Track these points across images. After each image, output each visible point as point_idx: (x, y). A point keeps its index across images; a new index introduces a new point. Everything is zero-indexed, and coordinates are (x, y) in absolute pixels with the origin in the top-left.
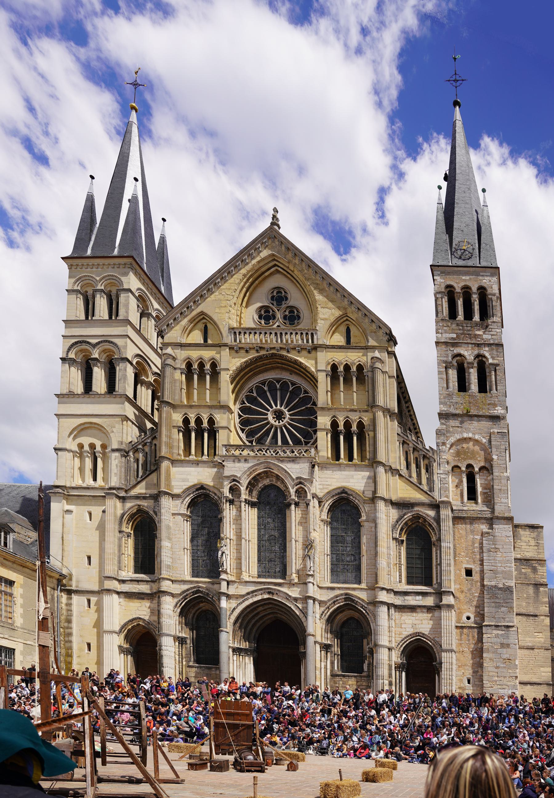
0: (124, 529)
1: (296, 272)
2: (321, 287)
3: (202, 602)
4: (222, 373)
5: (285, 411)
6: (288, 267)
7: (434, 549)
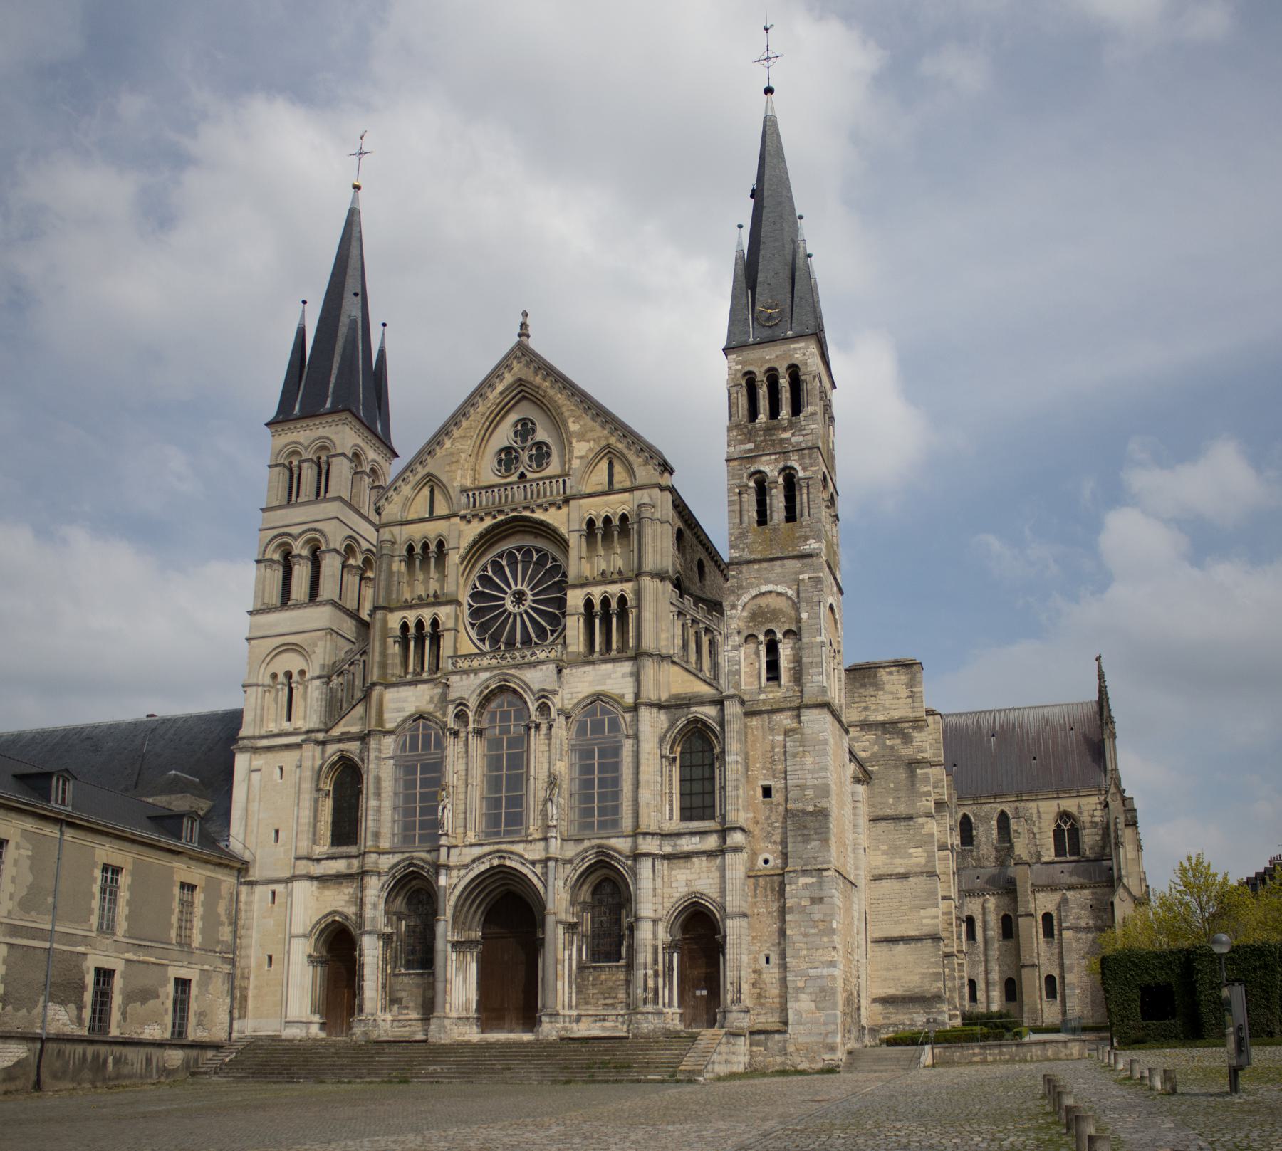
0: (321, 786)
3: (415, 878)
4: (451, 552)
5: (529, 593)
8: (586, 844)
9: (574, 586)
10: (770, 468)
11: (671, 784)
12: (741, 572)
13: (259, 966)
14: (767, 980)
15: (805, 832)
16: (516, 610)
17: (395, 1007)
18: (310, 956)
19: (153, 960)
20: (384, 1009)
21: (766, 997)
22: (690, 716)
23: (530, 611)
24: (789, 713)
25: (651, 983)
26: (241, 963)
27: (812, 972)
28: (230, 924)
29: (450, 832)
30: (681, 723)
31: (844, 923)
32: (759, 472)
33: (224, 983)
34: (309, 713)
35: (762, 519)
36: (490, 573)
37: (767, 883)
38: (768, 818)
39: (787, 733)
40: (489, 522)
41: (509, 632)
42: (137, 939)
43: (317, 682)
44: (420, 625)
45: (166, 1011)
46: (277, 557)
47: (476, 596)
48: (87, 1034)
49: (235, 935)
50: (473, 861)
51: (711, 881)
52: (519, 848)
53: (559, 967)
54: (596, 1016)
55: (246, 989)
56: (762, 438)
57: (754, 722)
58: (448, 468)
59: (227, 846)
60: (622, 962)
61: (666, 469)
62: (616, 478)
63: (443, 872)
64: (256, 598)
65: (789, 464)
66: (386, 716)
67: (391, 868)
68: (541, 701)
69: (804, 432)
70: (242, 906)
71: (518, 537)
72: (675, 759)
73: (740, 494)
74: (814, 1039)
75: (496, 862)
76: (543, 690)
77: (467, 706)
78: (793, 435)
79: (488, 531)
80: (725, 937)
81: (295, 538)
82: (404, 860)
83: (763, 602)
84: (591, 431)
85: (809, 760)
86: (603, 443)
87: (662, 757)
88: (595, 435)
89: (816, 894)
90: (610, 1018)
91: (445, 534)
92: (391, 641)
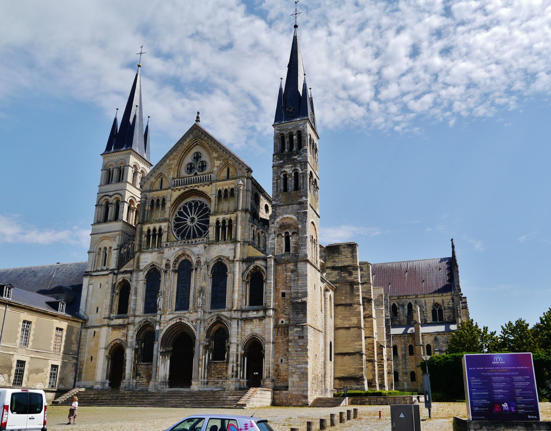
1: (205, 144)
2: (216, 150)
6: (202, 142)
7: (264, 284)
8: (213, 314)
9: (213, 215)
10: (288, 169)
11: (246, 291)
12: (276, 210)
13: (87, 360)
14: (281, 369)
15: (297, 311)
16: (191, 225)
17: (138, 377)
18: (107, 356)
19: (42, 357)
20: (133, 378)
21: (280, 376)
22: (254, 265)
23: (196, 225)
24: (293, 264)
25: (235, 369)
26: (81, 359)
27: (298, 366)
28: (77, 344)
29: (161, 309)
30: (251, 267)
31: (313, 346)
32: (285, 171)
33: (72, 367)
34: (113, 264)
35: (286, 189)
36: (182, 211)
37: (282, 330)
38: (284, 305)
39: (292, 271)
40: (182, 191)
41: (188, 233)
42: (36, 349)
43: (116, 251)
44: (155, 230)
45: (47, 377)
46: (104, 203)
47: (177, 219)
48: (12, 386)
49: (79, 348)
50: (170, 320)
51: (260, 329)
52: (187, 315)
53: (200, 362)
54: (214, 382)
55: (82, 369)
56: (286, 159)
57: (279, 268)
58: (168, 171)
59: (78, 314)
60: (225, 361)
61: (249, 171)
62: (230, 175)
63: (158, 324)
64: (94, 219)
65: (296, 168)
66: (141, 264)
67: (139, 322)
68: (198, 259)
69: (302, 156)
70: (82, 337)
71: (193, 197)
72: (248, 282)
73: (277, 180)
74: (299, 393)
75: (178, 321)
76: (198, 255)
77: (170, 261)
78: (298, 157)
79: (182, 195)
80: (265, 351)
81: (111, 196)
82: (143, 320)
83: (284, 221)
84: (221, 157)
85: (300, 282)
86: (226, 161)
87: (243, 280)
88: (223, 158)
89: (301, 335)
90: (220, 383)
91: (166, 196)
92: (143, 236)
